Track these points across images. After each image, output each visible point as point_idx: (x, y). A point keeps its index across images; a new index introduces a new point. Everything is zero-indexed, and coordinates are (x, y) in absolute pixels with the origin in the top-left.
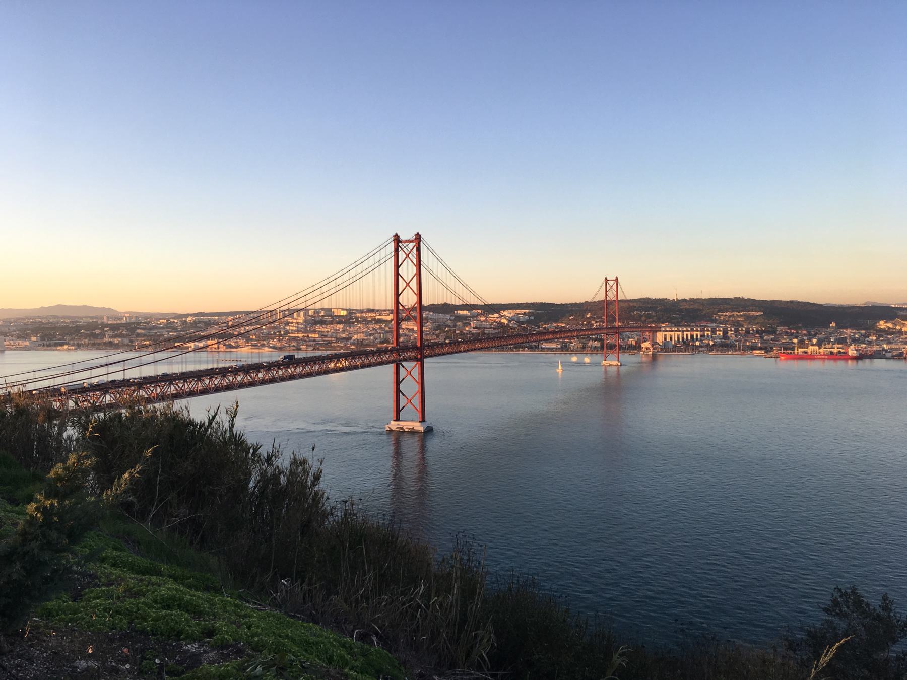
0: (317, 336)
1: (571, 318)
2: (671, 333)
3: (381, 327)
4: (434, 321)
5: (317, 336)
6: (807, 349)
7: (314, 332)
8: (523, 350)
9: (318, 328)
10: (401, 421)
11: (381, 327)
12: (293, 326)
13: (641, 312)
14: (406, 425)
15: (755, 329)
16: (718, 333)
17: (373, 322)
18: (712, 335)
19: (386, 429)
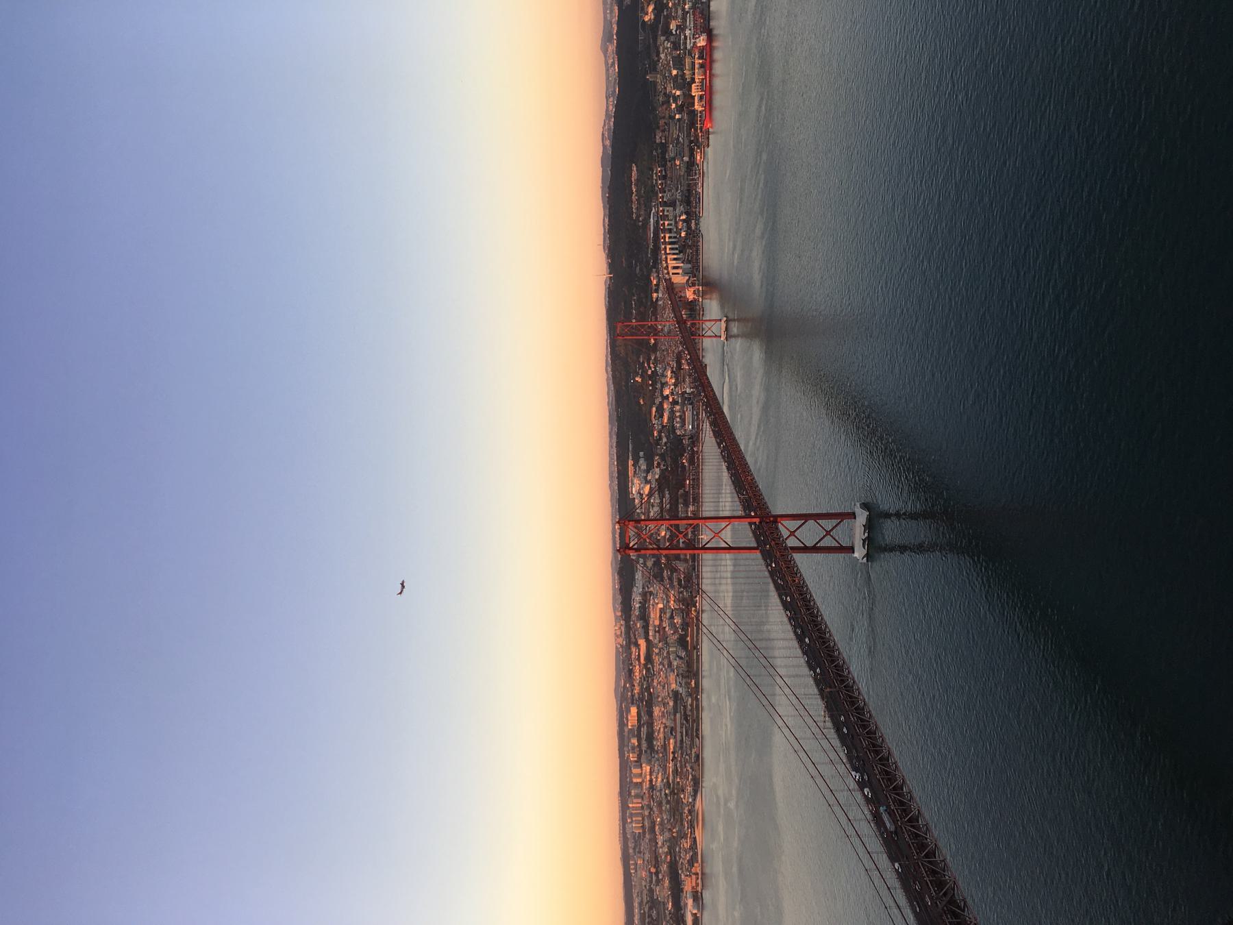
0: (672, 741)
1: (642, 403)
2: (670, 269)
3: (657, 654)
4: (648, 583)
5: (672, 741)
6: (696, 98)
7: (665, 747)
8: (697, 452)
9: (658, 744)
10: (852, 543)
11: (657, 654)
12: (657, 778)
13: (632, 313)
14: (859, 534)
15: (659, 169)
16: (666, 213)
17: (649, 666)
18: (668, 220)
19: (865, 561)
